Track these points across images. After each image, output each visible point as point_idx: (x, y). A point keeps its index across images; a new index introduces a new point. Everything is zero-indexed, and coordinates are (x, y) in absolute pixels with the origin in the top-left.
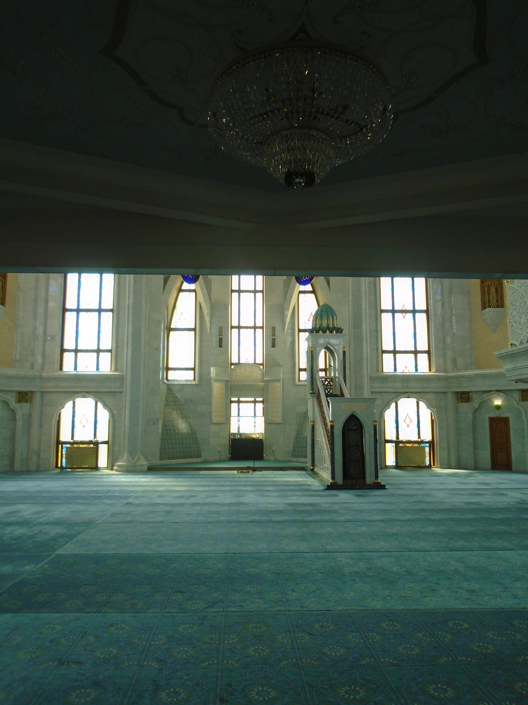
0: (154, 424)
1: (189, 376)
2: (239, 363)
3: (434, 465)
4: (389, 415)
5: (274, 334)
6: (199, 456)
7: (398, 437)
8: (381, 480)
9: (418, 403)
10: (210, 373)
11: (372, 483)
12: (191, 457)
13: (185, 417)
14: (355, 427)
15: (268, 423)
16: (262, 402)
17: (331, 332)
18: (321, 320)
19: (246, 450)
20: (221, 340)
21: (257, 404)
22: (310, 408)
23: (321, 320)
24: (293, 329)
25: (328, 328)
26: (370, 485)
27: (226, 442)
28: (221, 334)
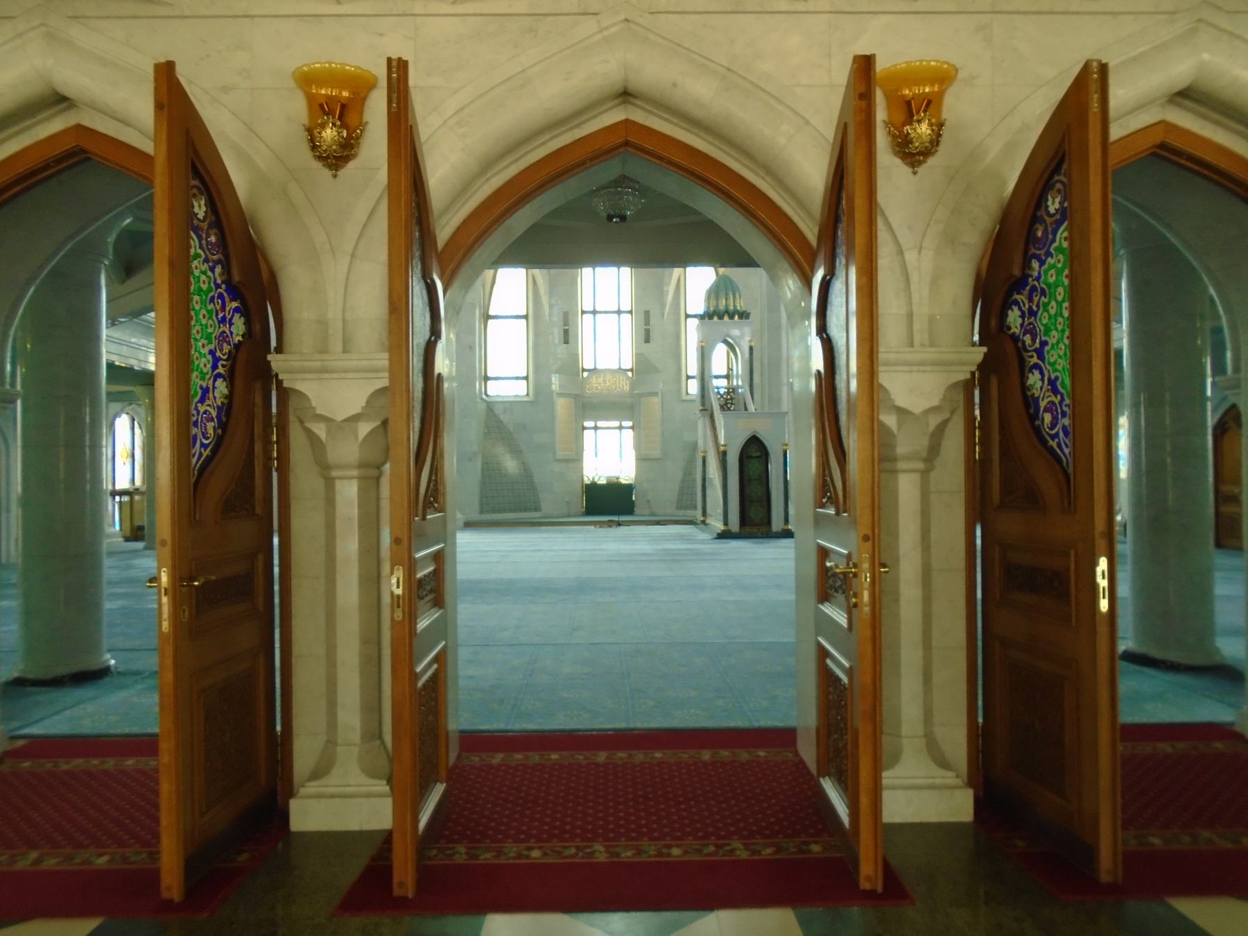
0: (470, 460)
1: (519, 390)
5: (647, 322)
6: (537, 509)
10: (551, 384)
12: (526, 510)
13: (515, 451)
15: (642, 459)
16: (632, 428)
17: (731, 317)
20: (566, 332)
22: (700, 433)
24: (678, 313)
25: (727, 312)
27: (579, 487)
28: (566, 323)
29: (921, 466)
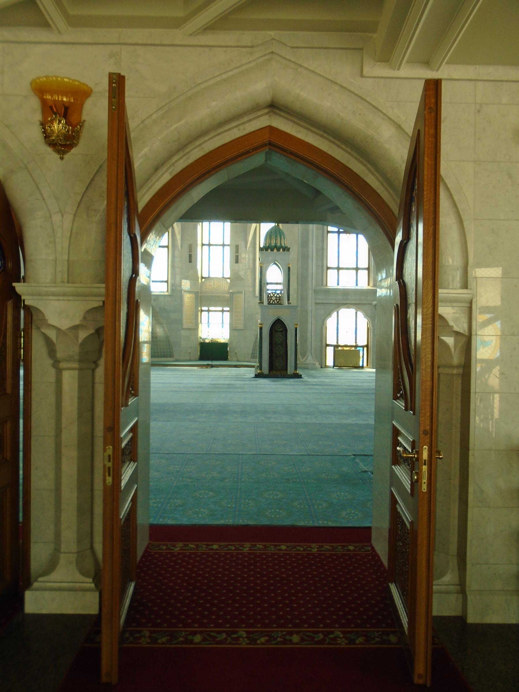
2: (209, 277)
3: (367, 366)
4: (331, 323)
6: (171, 356)
7: (337, 343)
8: (299, 372)
9: (356, 313)
11: (292, 373)
12: (164, 357)
14: (281, 330)
15: (233, 329)
17: (278, 250)
18: (271, 240)
19: (213, 353)
20: (190, 256)
21: (225, 313)
23: (271, 240)
26: (289, 375)
28: (190, 251)
29: (76, 365)
